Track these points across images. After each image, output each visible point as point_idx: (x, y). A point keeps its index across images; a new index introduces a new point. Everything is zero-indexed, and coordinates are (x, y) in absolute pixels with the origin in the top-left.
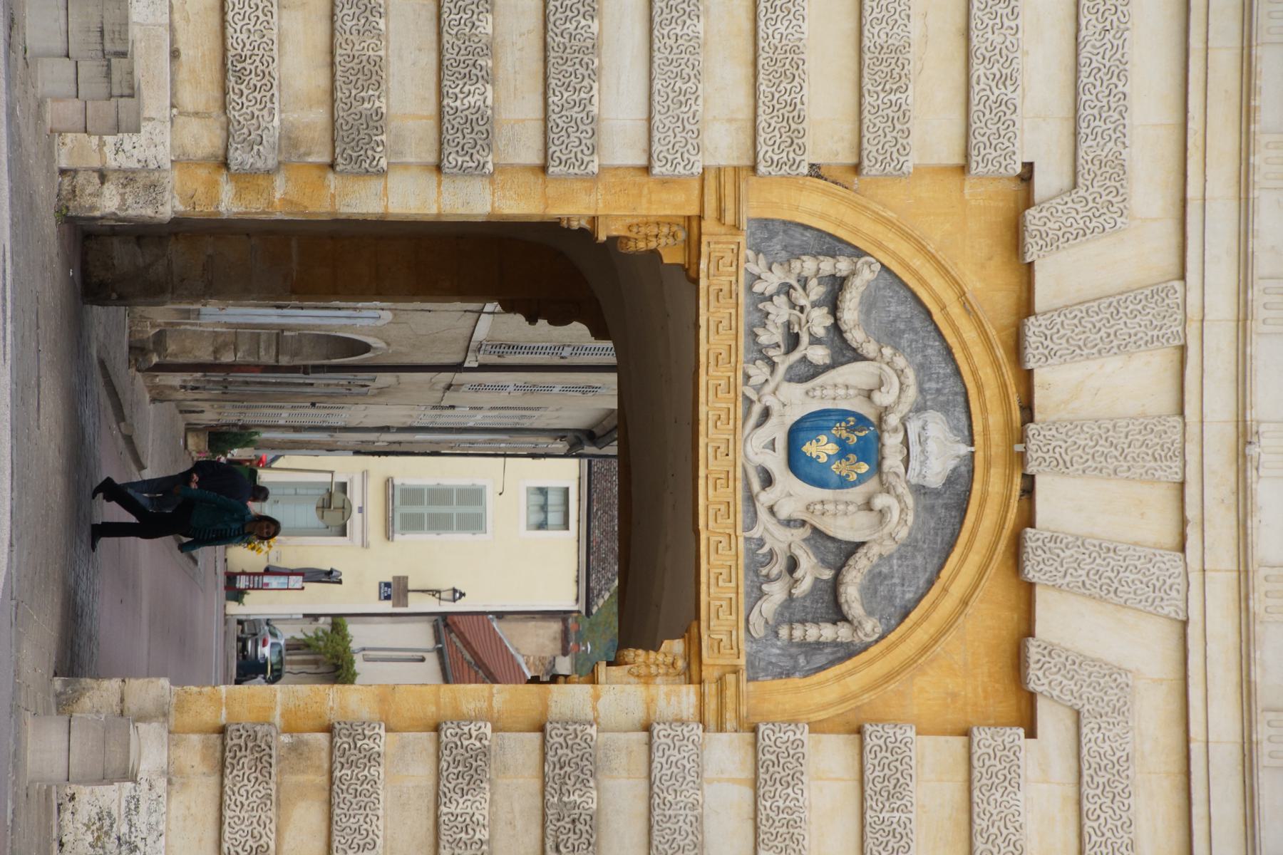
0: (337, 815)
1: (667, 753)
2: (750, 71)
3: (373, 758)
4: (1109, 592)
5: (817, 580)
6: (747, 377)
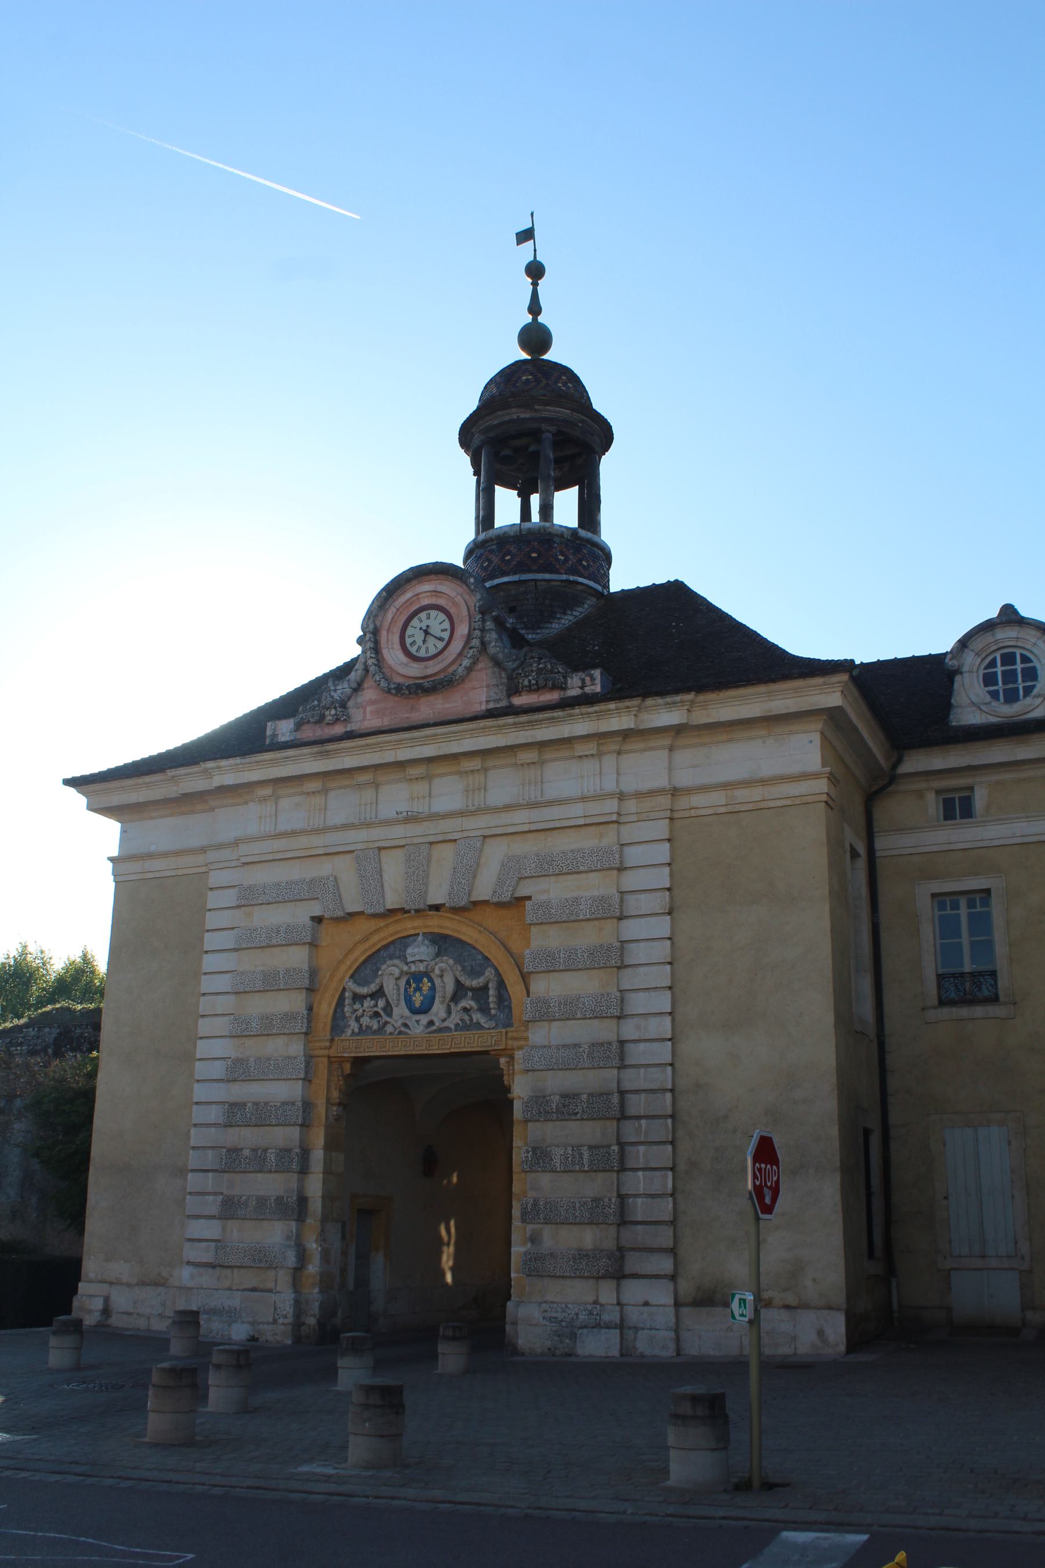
0: (560, 1220)
1: (535, 1063)
2: (270, 1037)
3: (536, 1203)
4: (471, 870)
5: (473, 999)
6: (391, 1034)
